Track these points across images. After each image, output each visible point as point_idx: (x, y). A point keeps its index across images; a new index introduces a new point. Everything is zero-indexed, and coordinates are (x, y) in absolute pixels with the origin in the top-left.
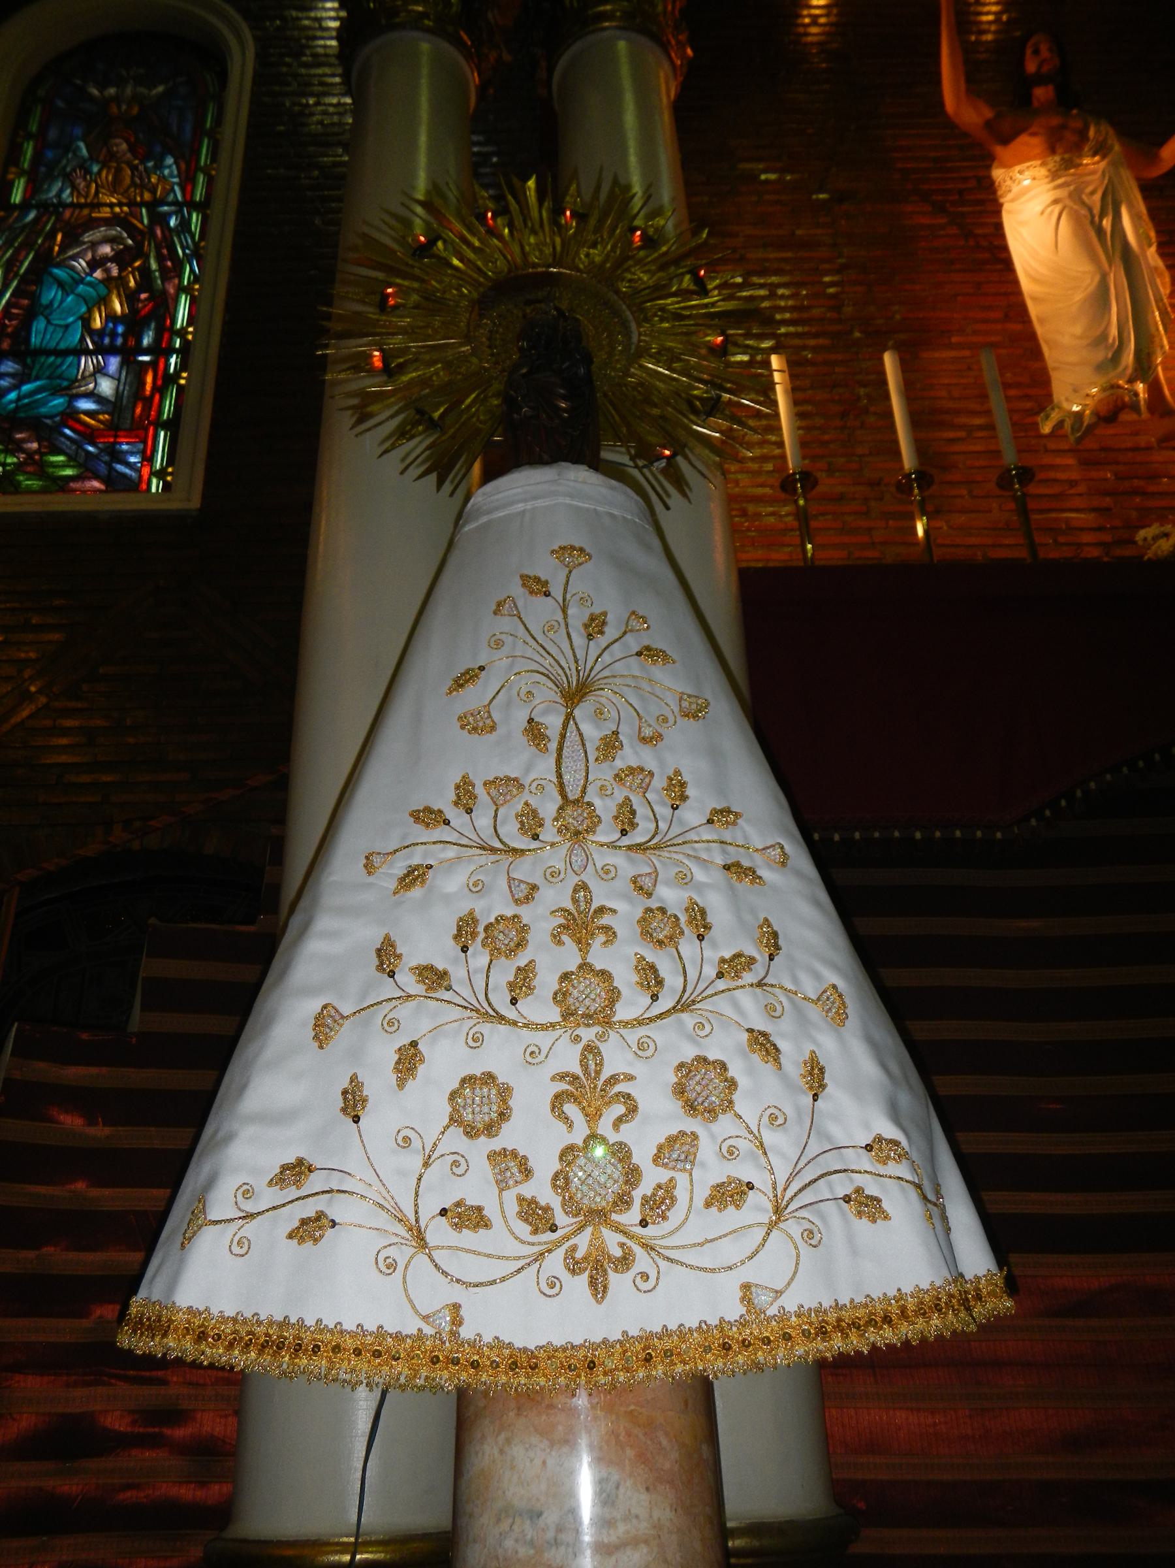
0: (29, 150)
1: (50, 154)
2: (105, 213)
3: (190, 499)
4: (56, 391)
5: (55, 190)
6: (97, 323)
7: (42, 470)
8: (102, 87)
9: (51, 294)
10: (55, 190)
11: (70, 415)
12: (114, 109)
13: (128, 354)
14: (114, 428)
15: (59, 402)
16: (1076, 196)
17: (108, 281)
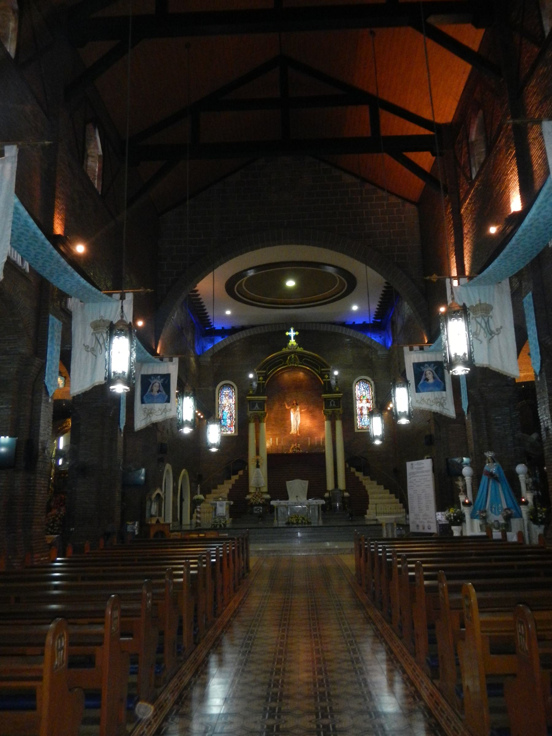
0: (220, 398)
1: (222, 399)
2: (226, 405)
3: (237, 434)
4: (226, 423)
5: (223, 403)
6: (228, 416)
7: (226, 430)
8: (225, 390)
9: (224, 414)
10: (223, 403)
11: (227, 425)
12: (226, 394)
13: (230, 419)
14: (230, 426)
15: (226, 424)
16: (294, 416)
17: (228, 412)
